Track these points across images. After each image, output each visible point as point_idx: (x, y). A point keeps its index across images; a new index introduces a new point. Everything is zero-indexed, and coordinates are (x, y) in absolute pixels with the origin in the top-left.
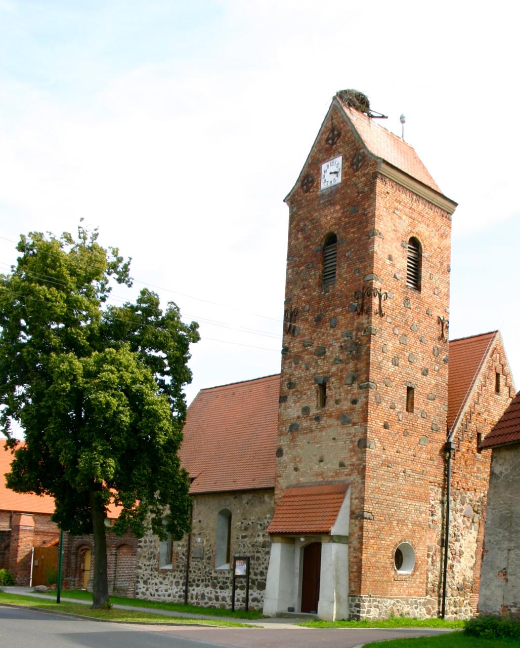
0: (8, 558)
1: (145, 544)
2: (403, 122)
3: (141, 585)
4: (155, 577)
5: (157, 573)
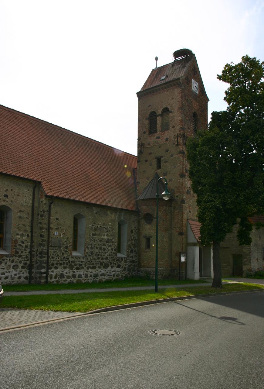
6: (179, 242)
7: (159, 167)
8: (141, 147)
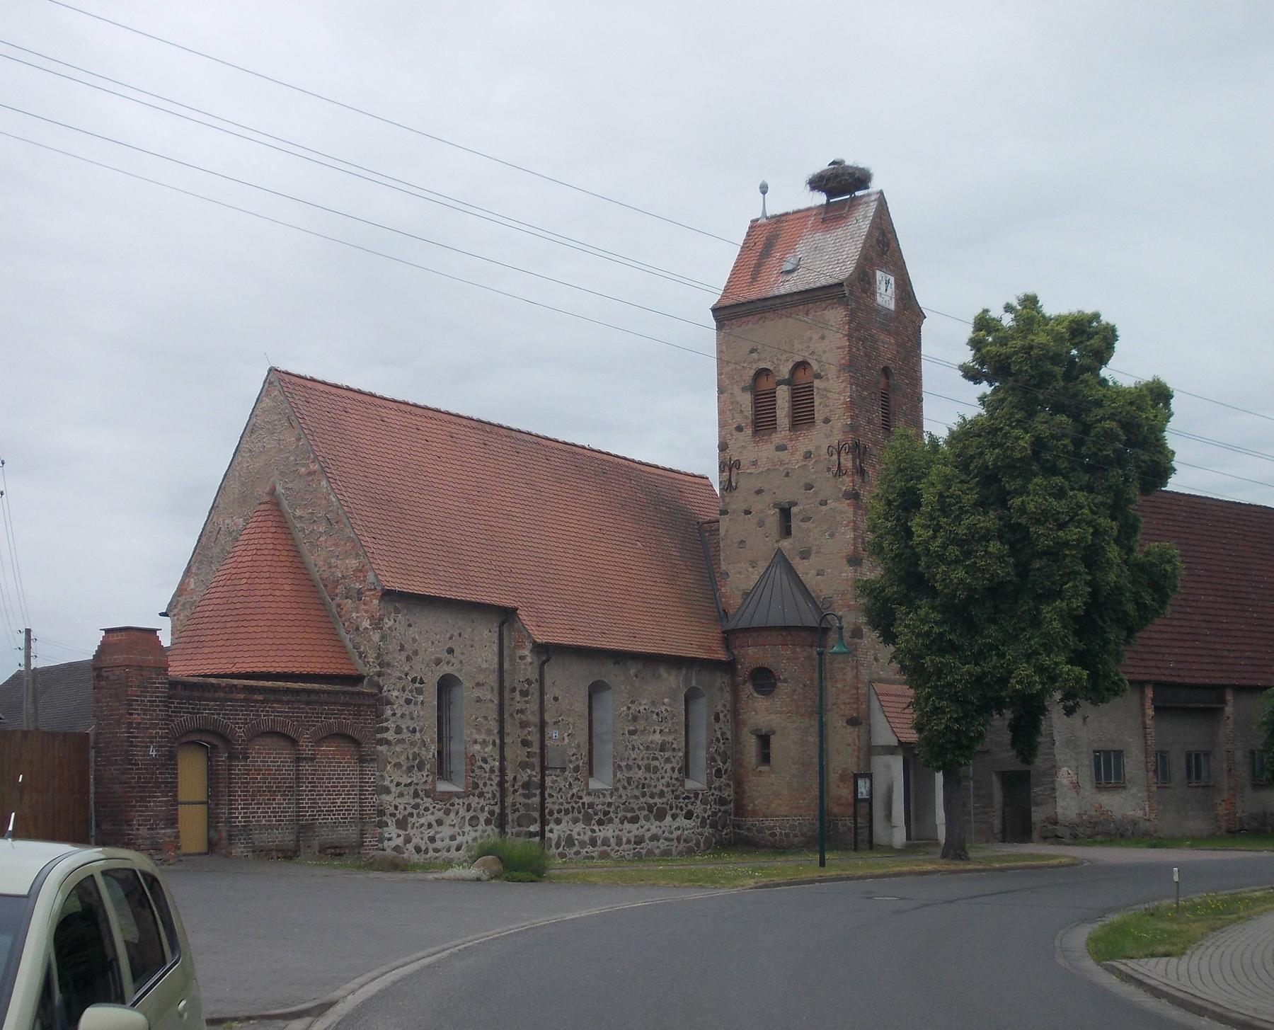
0: (793, 827)
1: (399, 737)
2: (764, 193)
3: (392, 830)
4: (426, 809)
5: (430, 800)
6: (848, 745)
7: (786, 531)
8: (730, 470)
